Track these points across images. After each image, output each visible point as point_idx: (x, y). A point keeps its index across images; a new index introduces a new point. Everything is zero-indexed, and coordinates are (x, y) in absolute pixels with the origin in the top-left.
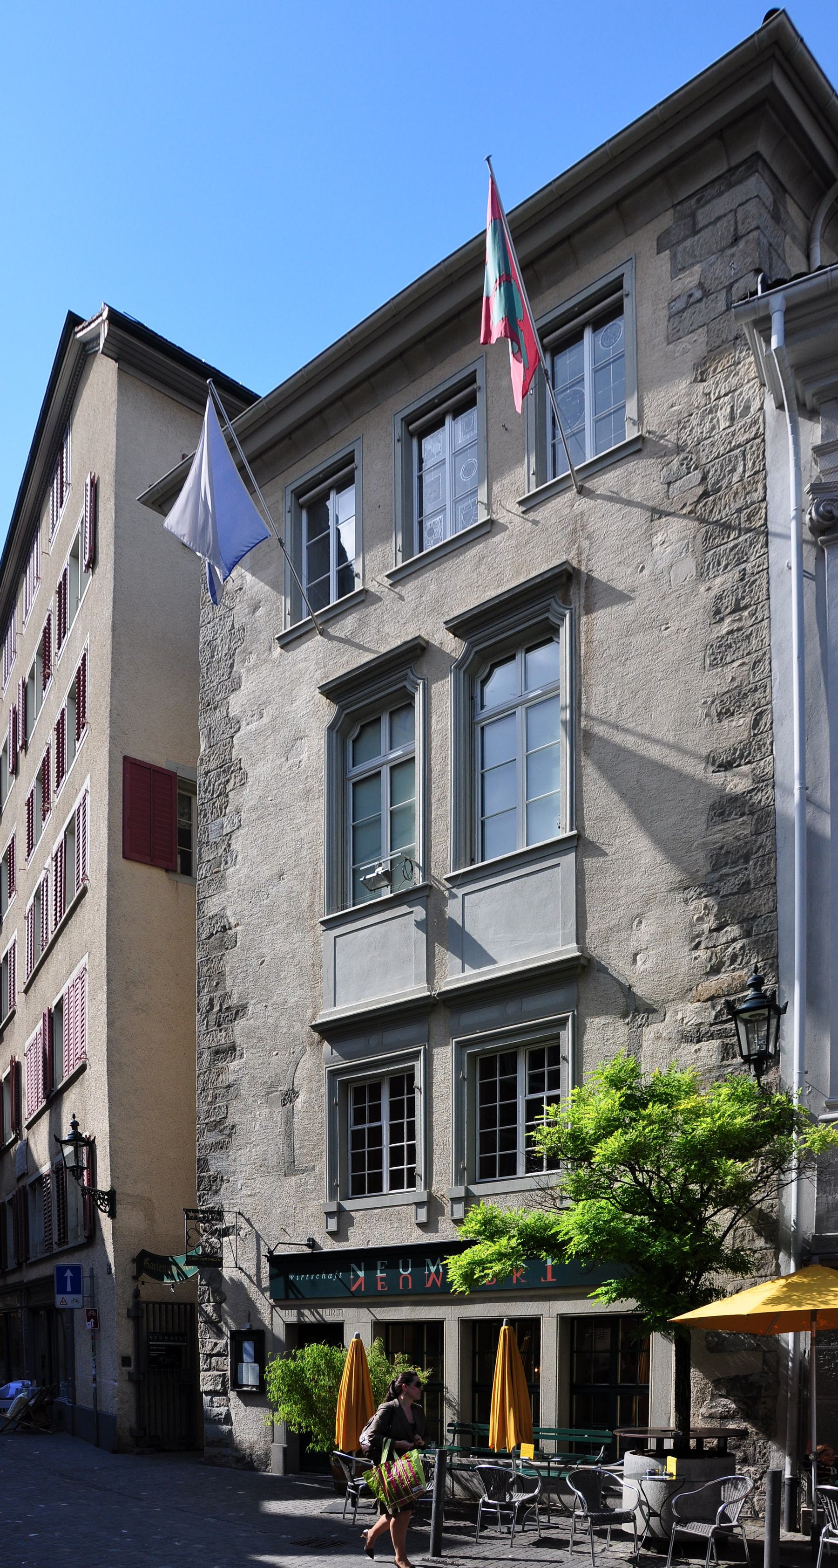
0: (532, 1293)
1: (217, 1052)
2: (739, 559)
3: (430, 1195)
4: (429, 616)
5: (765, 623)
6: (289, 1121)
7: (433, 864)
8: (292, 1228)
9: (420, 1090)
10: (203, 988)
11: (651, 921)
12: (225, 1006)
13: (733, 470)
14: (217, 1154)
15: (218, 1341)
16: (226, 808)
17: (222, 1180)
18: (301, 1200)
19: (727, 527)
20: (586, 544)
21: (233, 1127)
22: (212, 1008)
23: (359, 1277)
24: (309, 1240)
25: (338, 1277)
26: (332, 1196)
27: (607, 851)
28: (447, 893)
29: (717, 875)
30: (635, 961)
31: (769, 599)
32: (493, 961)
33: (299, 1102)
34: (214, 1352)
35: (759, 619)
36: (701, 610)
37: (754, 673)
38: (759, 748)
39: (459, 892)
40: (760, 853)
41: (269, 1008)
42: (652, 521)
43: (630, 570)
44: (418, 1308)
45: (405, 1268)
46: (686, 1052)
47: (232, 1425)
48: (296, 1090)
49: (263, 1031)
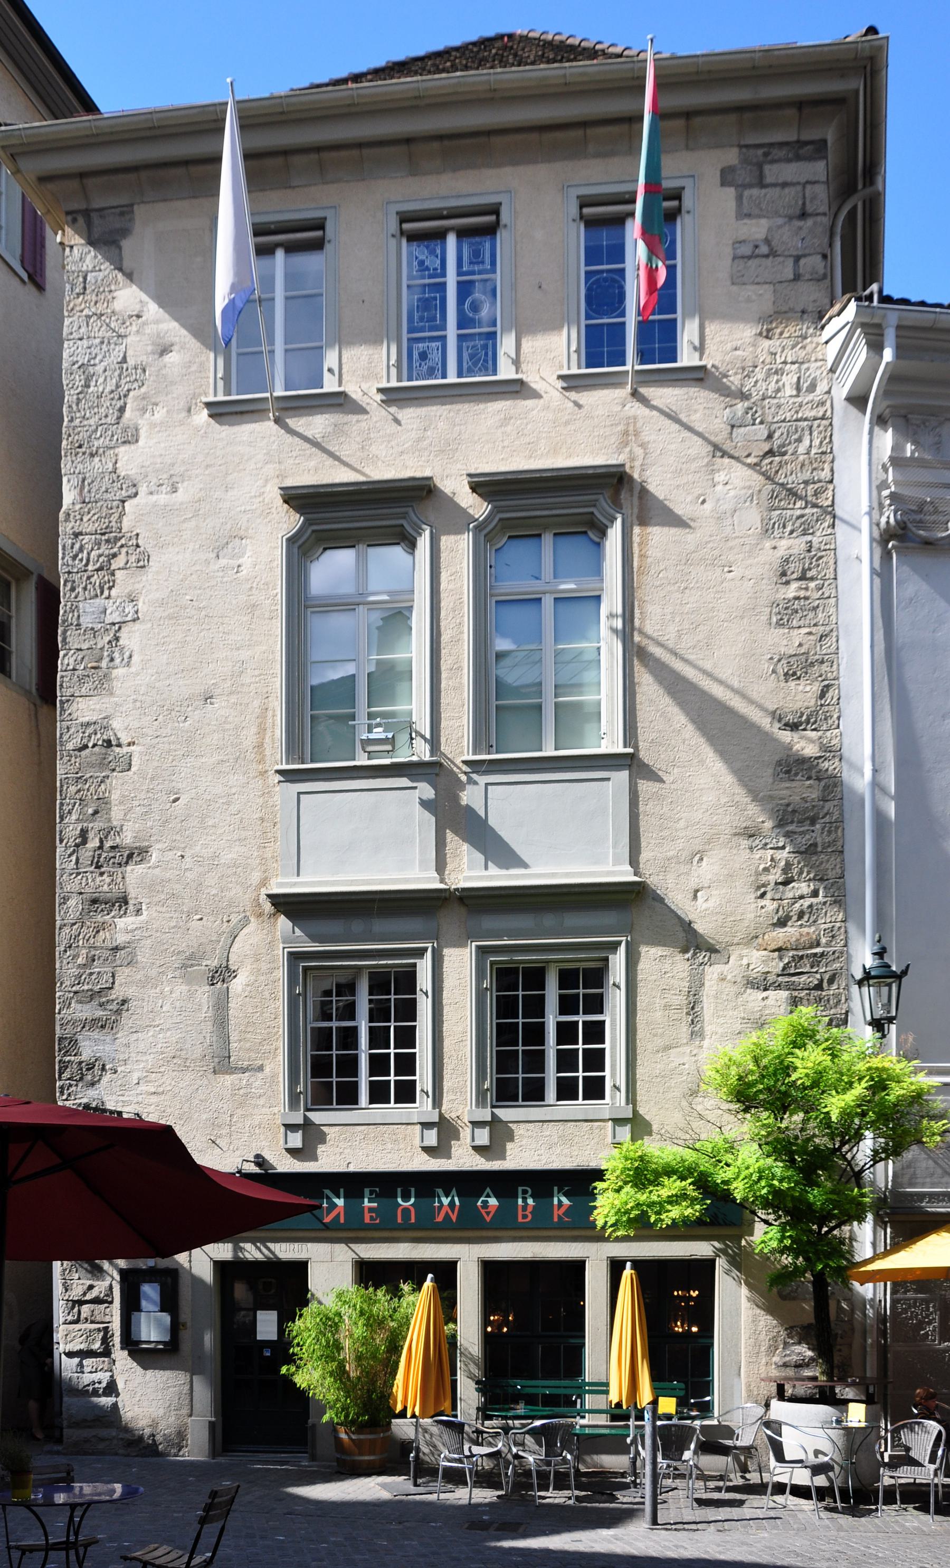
0: (576, 1233)
1: (94, 901)
2: (804, 530)
4: (436, 456)
5: (833, 601)
6: (221, 1006)
7: (443, 740)
8: (227, 1140)
9: (426, 994)
10: (70, 812)
11: (714, 860)
12: (108, 844)
13: (799, 440)
14: (96, 1034)
15: (95, 1283)
16: (110, 588)
17: (103, 1068)
18: (241, 1105)
19: (792, 493)
20: (639, 452)
21: (124, 1002)
22: (84, 841)
23: (336, 1205)
24: (258, 1156)
27: (665, 779)
28: (464, 778)
30: (695, 897)
31: (836, 579)
32: (525, 865)
33: (237, 985)
34: (88, 1297)
35: (826, 595)
36: (767, 566)
37: (821, 646)
38: (826, 719)
39: (482, 780)
40: (827, 819)
41: (187, 859)
42: (714, 457)
43: (689, 499)
44: (421, 1245)
45: (406, 1197)
46: (752, 998)
47: (118, 1395)
48: (233, 968)
49: (177, 886)
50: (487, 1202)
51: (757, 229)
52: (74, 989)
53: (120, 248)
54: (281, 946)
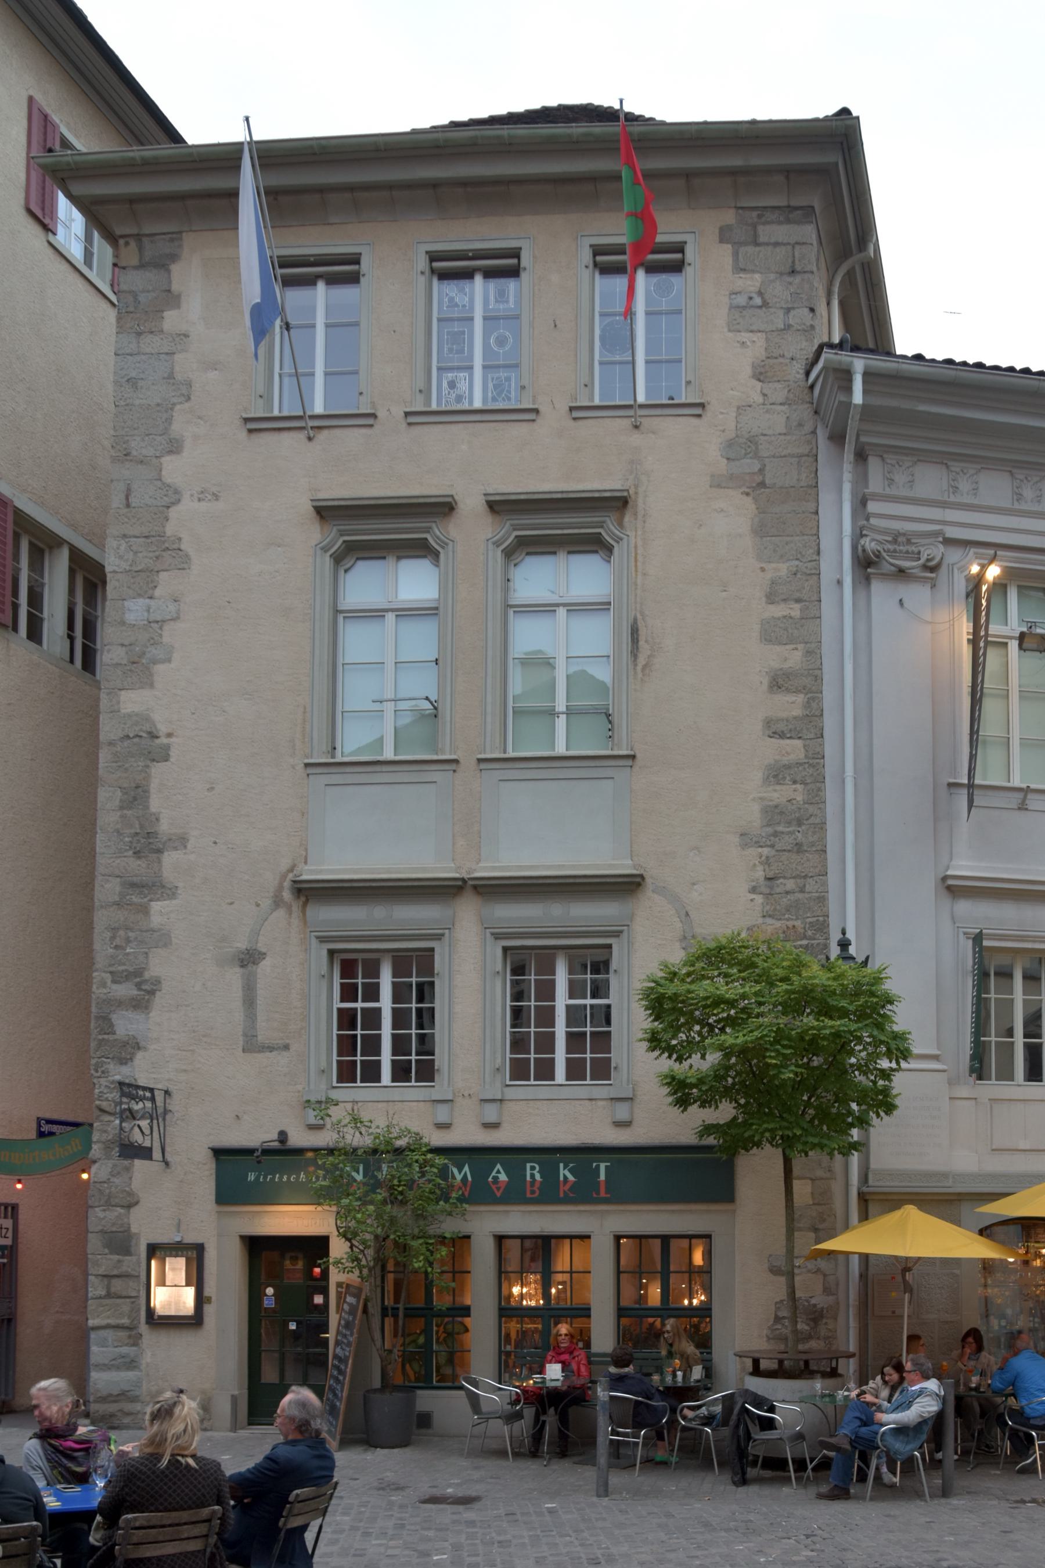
14: (130, 1014)
29: (770, 830)
33: (265, 967)
50: (497, 1178)
51: (751, 282)
52: (111, 969)
53: (169, 271)
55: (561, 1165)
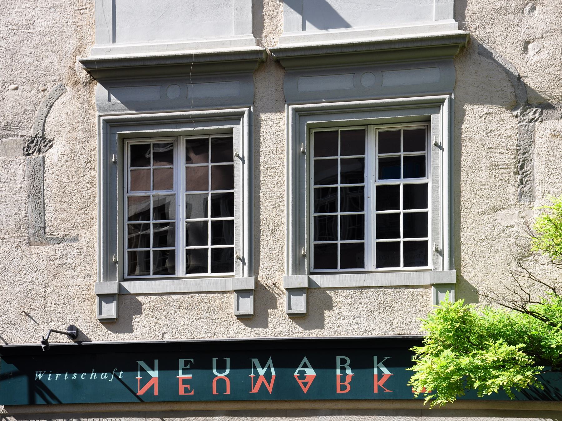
3: (257, 283)
6: (37, 177)
9: (242, 159)
11: (548, 8)
23: (150, 377)
25: (116, 377)
26: (109, 270)
33: (53, 155)
45: (221, 367)
48: (49, 137)
54: (97, 114)
55: (375, 358)
